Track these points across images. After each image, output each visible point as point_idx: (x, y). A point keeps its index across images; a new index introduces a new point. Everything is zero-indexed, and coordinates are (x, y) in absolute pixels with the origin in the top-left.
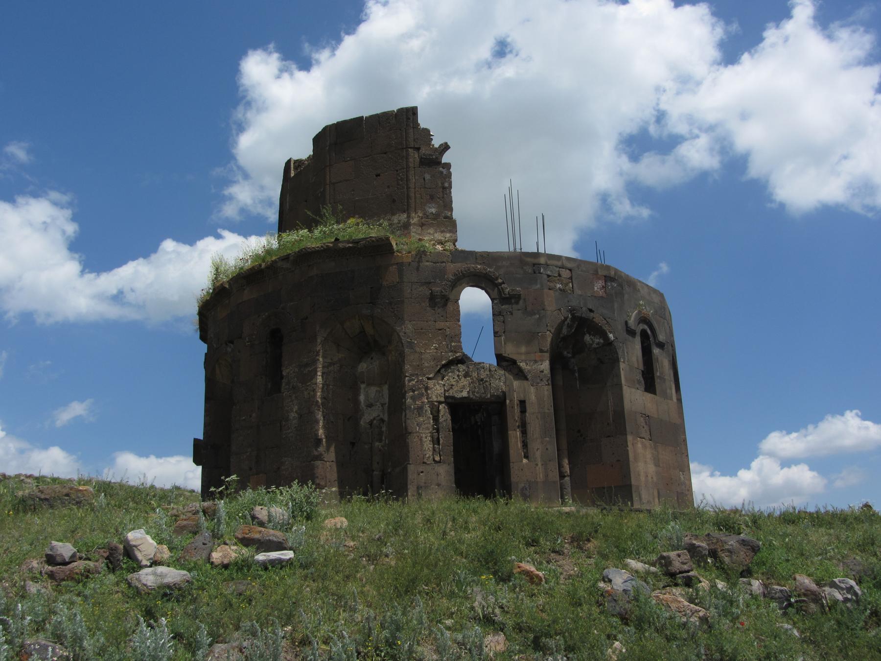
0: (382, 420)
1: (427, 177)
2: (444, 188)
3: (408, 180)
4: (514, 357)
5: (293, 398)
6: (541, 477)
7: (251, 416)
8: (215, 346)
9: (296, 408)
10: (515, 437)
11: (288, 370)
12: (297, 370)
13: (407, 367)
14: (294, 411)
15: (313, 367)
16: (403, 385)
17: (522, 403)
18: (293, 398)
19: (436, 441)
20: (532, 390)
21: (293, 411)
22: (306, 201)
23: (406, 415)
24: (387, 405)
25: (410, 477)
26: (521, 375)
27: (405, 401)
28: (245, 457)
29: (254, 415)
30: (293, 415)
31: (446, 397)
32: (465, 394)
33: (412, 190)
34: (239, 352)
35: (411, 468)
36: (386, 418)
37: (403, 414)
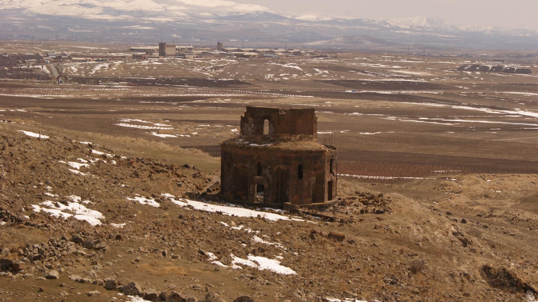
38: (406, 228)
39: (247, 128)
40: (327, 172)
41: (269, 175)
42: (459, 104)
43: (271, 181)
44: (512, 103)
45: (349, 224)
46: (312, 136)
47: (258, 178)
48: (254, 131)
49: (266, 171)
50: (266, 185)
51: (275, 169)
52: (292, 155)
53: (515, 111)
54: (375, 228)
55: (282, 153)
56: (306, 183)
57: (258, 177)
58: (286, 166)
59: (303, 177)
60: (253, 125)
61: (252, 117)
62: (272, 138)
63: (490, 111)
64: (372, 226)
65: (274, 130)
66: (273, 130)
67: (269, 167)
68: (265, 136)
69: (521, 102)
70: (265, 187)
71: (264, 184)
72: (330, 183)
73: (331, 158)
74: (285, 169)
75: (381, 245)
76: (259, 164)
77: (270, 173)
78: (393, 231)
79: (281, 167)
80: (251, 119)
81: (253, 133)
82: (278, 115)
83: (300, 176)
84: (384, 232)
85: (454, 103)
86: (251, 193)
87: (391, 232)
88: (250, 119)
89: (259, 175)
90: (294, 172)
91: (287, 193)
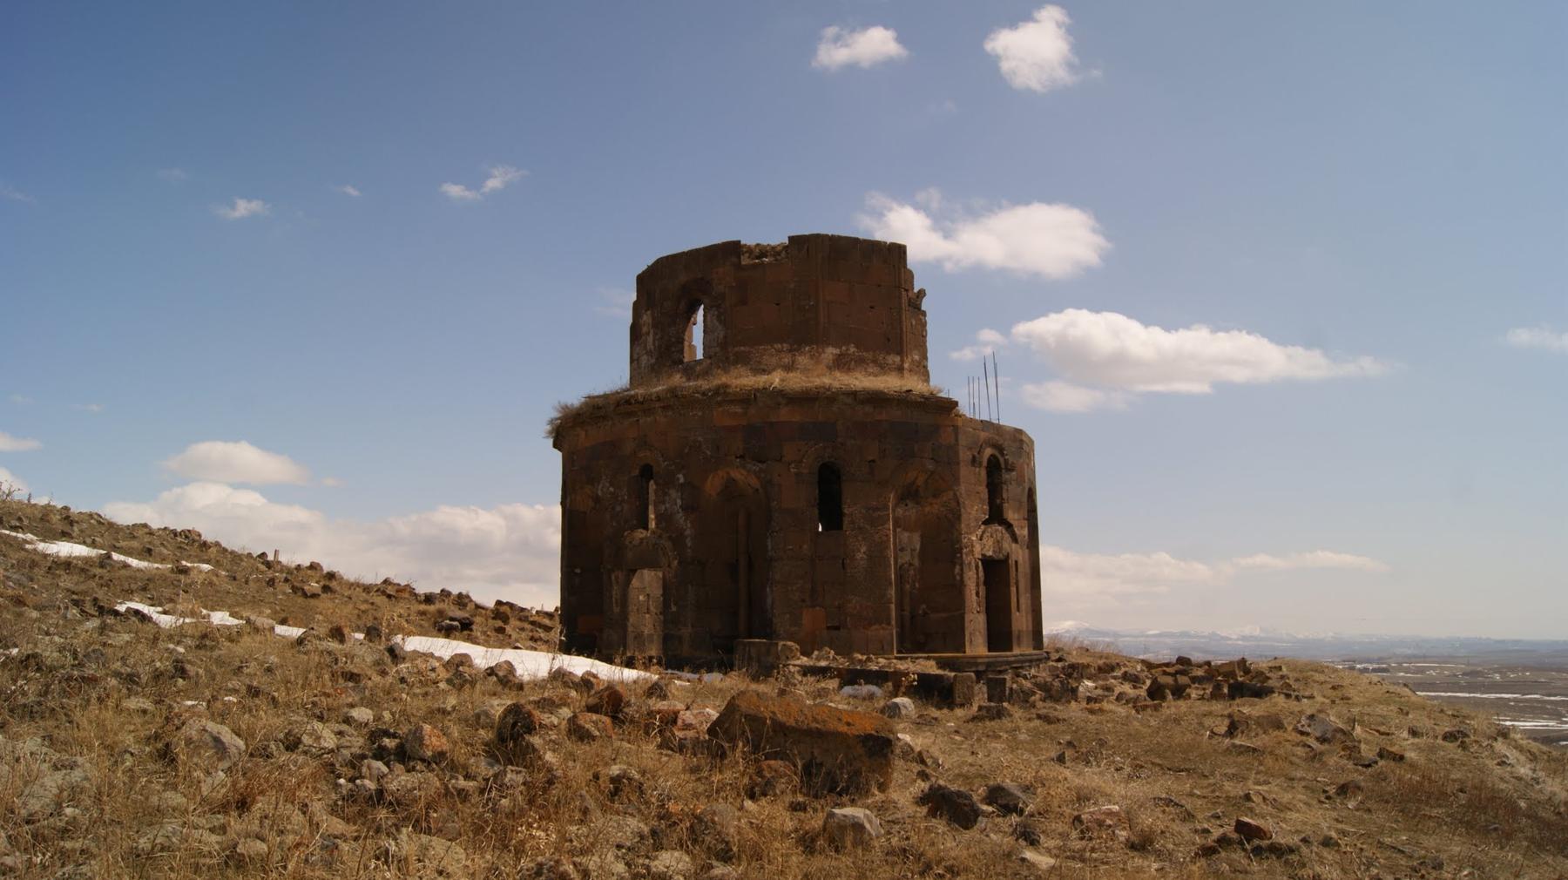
0: (911, 565)
1: (914, 323)
2: (923, 336)
3: (901, 322)
4: (1012, 522)
5: (860, 538)
6: (1025, 629)
7: (801, 547)
8: (709, 453)
9: (863, 549)
10: (1013, 589)
11: (850, 510)
12: (864, 511)
13: (963, 525)
14: (862, 551)
15: (885, 513)
16: (959, 541)
17: (1016, 562)
18: (860, 538)
19: (977, 594)
20: (1020, 551)
21: (860, 551)
22: (777, 304)
23: (962, 570)
24: (918, 551)
25: (967, 624)
26: (1015, 539)
27: (961, 556)
28: (794, 588)
29: (805, 546)
30: (859, 556)
31: (982, 555)
32: (990, 553)
33: (905, 334)
34: (779, 475)
35: (966, 616)
36: (916, 562)
37: (958, 567)
38: (1439, 741)
40: (975, 510)
41: (680, 517)
43: (689, 542)
45: (1044, 707)
46: (897, 359)
47: (642, 539)
51: (712, 485)
52: (785, 414)
54: (1232, 730)
55: (739, 410)
56: (861, 554)
58: (756, 467)
59: (846, 521)
64: (1208, 722)
65: (721, 336)
66: (720, 333)
67: (682, 480)
72: (995, 570)
73: (988, 452)
74: (754, 482)
75: (1327, 843)
77: (685, 508)
78: (1367, 751)
79: (738, 475)
82: (739, 266)
83: (832, 514)
84: (1300, 751)
86: (617, 610)
87: (1351, 750)
90: (796, 495)
91: (769, 601)
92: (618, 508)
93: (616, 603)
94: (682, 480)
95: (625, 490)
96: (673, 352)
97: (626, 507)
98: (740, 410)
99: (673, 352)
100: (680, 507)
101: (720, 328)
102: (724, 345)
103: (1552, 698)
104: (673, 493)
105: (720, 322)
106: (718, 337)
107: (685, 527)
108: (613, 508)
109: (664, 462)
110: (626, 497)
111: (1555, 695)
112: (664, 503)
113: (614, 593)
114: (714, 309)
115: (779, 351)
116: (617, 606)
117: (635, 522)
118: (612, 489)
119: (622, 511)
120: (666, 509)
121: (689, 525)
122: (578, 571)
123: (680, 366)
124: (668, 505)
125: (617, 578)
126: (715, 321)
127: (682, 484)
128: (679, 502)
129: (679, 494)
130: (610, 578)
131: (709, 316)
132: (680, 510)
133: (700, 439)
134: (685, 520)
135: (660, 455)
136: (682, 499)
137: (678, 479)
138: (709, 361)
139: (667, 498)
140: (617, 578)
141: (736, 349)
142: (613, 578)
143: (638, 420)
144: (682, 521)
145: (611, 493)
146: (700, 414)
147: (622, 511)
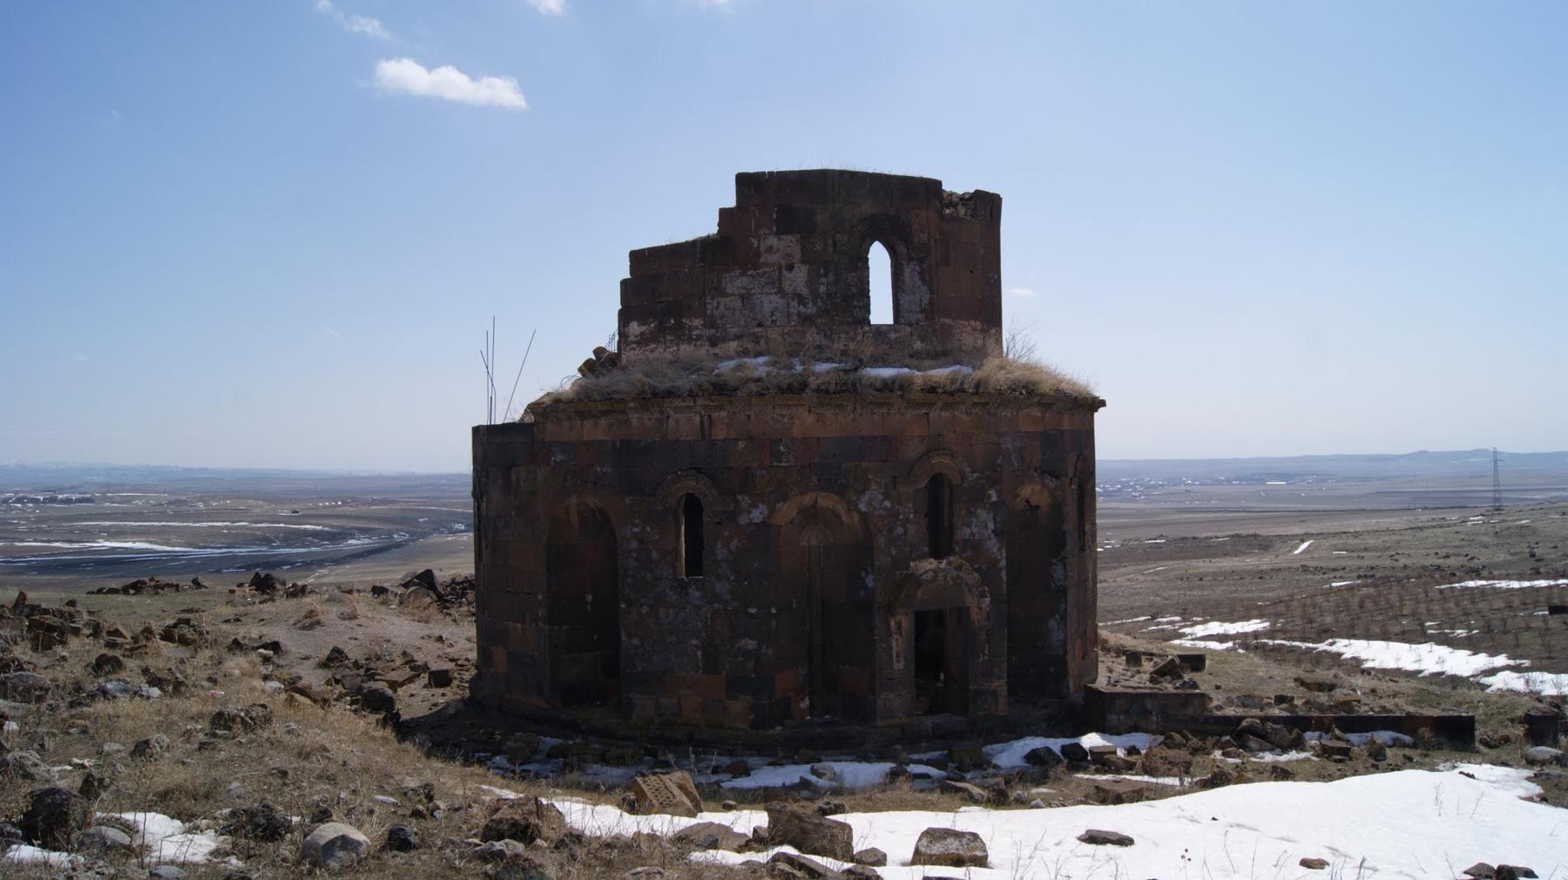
22: (971, 272)
39: (742, 297)
42: (23, 541)
44: (91, 534)
47: (936, 572)
48: (811, 310)
49: (980, 526)
50: (980, 607)
53: (98, 542)
57: (930, 564)
58: (1052, 483)
60: (798, 278)
61: (779, 233)
62: (918, 345)
63: (66, 545)
67: (994, 499)
68: (880, 330)
69: (100, 532)
70: (976, 616)
71: (971, 601)
76: (937, 481)
80: (778, 246)
81: (806, 320)
85: (14, 540)
88: (773, 241)
89: (936, 554)
91: (1056, 636)
92: (900, 530)
93: (897, 656)
94: (994, 499)
95: (911, 506)
96: (856, 307)
97: (912, 529)
98: (1039, 414)
99: (856, 307)
100: (993, 531)
101: (924, 288)
102: (931, 312)
103: (260, 525)
104: (983, 514)
105: (922, 278)
106: (921, 301)
107: (999, 557)
108: (891, 530)
109: (973, 472)
110: (911, 516)
111: (261, 522)
112: (969, 525)
113: (894, 644)
114: (915, 262)
115: (974, 330)
116: (898, 662)
117: (926, 549)
118: (887, 504)
119: (905, 533)
120: (972, 534)
121: (1004, 555)
122: (774, 611)
123: (867, 328)
124: (975, 530)
125: (899, 624)
126: (917, 279)
127: (994, 503)
128: (991, 526)
129: (991, 515)
130: (888, 624)
131: (907, 272)
132: (992, 536)
133: (1010, 448)
134: (1000, 549)
135: (966, 464)
136: (995, 523)
137: (990, 497)
138: (909, 329)
139: (974, 519)
140: (899, 624)
141: (942, 320)
142: (893, 624)
143: (926, 413)
144: (995, 550)
145: (885, 509)
146: (1009, 415)
147: (905, 533)
